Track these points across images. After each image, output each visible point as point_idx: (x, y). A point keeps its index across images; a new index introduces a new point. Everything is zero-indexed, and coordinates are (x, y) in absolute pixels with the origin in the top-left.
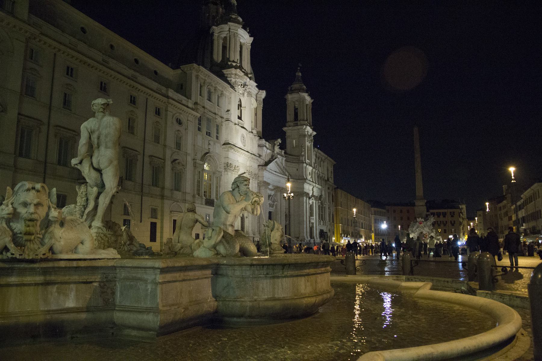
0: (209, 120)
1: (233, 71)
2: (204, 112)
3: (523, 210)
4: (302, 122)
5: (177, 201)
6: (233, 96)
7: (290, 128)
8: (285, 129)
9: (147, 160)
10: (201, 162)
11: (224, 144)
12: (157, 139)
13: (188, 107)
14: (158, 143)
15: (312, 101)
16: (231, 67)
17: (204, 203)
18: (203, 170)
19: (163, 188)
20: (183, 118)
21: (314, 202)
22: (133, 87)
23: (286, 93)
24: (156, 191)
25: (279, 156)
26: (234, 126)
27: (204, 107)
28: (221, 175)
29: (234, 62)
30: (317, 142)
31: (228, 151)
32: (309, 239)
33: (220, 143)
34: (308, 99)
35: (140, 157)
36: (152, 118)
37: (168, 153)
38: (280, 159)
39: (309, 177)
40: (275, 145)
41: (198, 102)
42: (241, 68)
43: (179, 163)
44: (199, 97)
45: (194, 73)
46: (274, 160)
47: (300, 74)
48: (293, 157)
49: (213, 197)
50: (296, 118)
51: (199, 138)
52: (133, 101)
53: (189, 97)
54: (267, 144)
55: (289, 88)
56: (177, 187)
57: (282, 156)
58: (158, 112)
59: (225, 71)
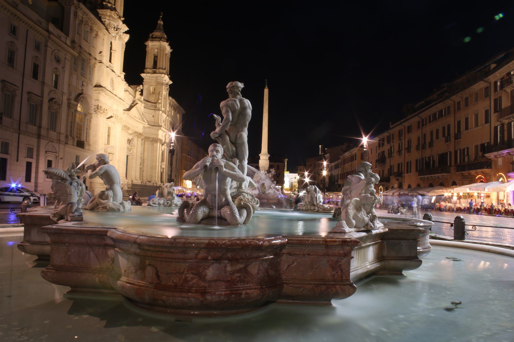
0: (83, 60)
1: (108, 12)
2: (80, 52)
3: (340, 169)
4: (161, 71)
5: (52, 142)
6: (106, 37)
7: (148, 75)
8: (143, 75)
9: (25, 96)
10: (76, 103)
11: (96, 86)
12: (35, 75)
13: (66, 44)
14: (37, 79)
15: (171, 51)
16: (106, 8)
17: (75, 144)
18: (76, 111)
19: (40, 127)
20: (62, 55)
21: (166, 148)
22: (15, 15)
23: (147, 40)
24: (33, 129)
25: (139, 102)
26: (106, 69)
27: (80, 46)
28: (92, 117)
29: (109, 2)
30: (173, 92)
31: (99, 93)
32: (160, 183)
33: (92, 85)
34: (168, 49)
35: (19, 93)
36: (31, 53)
37: (46, 91)
38: (140, 106)
39: (163, 125)
40: (136, 90)
41: (76, 40)
42: (115, 9)
43: (55, 102)
44: (77, 35)
45: (73, 9)
46: (135, 105)
47: (162, 23)
48: (152, 104)
49: (83, 138)
50: (155, 65)
51: (74, 77)
52: (13, 31)
53: (67, 34)
54: (130, 89)
55: (151, 35)
56: (53, 125)
57: (141, 101)
58: (37, 48)
59: (100, 11)
